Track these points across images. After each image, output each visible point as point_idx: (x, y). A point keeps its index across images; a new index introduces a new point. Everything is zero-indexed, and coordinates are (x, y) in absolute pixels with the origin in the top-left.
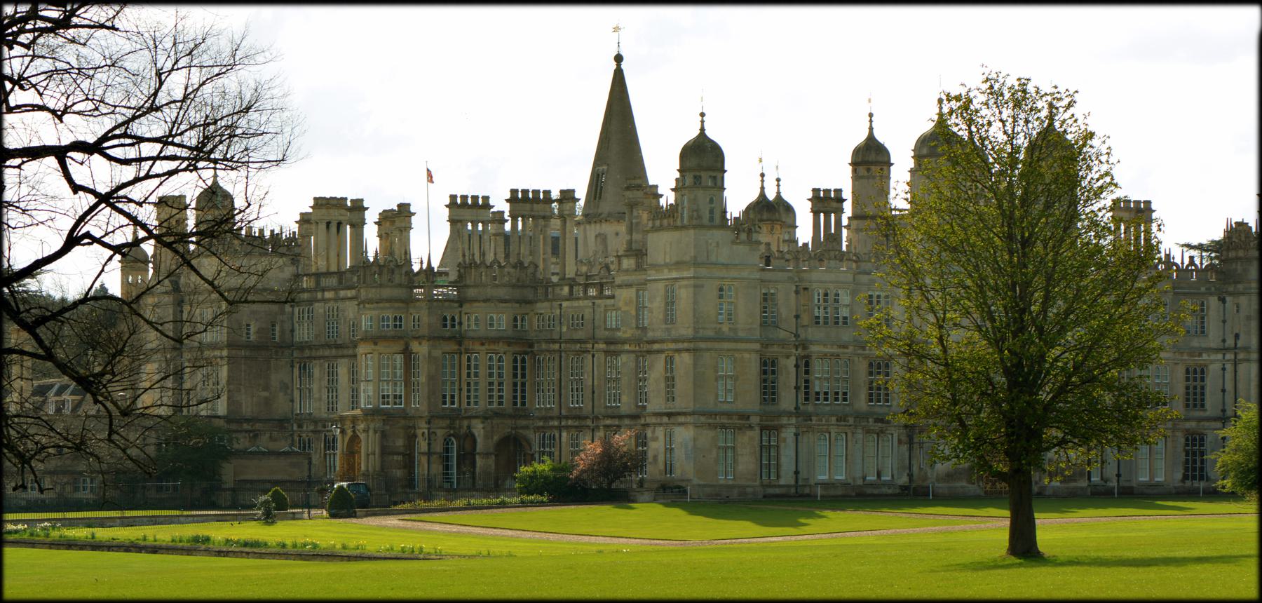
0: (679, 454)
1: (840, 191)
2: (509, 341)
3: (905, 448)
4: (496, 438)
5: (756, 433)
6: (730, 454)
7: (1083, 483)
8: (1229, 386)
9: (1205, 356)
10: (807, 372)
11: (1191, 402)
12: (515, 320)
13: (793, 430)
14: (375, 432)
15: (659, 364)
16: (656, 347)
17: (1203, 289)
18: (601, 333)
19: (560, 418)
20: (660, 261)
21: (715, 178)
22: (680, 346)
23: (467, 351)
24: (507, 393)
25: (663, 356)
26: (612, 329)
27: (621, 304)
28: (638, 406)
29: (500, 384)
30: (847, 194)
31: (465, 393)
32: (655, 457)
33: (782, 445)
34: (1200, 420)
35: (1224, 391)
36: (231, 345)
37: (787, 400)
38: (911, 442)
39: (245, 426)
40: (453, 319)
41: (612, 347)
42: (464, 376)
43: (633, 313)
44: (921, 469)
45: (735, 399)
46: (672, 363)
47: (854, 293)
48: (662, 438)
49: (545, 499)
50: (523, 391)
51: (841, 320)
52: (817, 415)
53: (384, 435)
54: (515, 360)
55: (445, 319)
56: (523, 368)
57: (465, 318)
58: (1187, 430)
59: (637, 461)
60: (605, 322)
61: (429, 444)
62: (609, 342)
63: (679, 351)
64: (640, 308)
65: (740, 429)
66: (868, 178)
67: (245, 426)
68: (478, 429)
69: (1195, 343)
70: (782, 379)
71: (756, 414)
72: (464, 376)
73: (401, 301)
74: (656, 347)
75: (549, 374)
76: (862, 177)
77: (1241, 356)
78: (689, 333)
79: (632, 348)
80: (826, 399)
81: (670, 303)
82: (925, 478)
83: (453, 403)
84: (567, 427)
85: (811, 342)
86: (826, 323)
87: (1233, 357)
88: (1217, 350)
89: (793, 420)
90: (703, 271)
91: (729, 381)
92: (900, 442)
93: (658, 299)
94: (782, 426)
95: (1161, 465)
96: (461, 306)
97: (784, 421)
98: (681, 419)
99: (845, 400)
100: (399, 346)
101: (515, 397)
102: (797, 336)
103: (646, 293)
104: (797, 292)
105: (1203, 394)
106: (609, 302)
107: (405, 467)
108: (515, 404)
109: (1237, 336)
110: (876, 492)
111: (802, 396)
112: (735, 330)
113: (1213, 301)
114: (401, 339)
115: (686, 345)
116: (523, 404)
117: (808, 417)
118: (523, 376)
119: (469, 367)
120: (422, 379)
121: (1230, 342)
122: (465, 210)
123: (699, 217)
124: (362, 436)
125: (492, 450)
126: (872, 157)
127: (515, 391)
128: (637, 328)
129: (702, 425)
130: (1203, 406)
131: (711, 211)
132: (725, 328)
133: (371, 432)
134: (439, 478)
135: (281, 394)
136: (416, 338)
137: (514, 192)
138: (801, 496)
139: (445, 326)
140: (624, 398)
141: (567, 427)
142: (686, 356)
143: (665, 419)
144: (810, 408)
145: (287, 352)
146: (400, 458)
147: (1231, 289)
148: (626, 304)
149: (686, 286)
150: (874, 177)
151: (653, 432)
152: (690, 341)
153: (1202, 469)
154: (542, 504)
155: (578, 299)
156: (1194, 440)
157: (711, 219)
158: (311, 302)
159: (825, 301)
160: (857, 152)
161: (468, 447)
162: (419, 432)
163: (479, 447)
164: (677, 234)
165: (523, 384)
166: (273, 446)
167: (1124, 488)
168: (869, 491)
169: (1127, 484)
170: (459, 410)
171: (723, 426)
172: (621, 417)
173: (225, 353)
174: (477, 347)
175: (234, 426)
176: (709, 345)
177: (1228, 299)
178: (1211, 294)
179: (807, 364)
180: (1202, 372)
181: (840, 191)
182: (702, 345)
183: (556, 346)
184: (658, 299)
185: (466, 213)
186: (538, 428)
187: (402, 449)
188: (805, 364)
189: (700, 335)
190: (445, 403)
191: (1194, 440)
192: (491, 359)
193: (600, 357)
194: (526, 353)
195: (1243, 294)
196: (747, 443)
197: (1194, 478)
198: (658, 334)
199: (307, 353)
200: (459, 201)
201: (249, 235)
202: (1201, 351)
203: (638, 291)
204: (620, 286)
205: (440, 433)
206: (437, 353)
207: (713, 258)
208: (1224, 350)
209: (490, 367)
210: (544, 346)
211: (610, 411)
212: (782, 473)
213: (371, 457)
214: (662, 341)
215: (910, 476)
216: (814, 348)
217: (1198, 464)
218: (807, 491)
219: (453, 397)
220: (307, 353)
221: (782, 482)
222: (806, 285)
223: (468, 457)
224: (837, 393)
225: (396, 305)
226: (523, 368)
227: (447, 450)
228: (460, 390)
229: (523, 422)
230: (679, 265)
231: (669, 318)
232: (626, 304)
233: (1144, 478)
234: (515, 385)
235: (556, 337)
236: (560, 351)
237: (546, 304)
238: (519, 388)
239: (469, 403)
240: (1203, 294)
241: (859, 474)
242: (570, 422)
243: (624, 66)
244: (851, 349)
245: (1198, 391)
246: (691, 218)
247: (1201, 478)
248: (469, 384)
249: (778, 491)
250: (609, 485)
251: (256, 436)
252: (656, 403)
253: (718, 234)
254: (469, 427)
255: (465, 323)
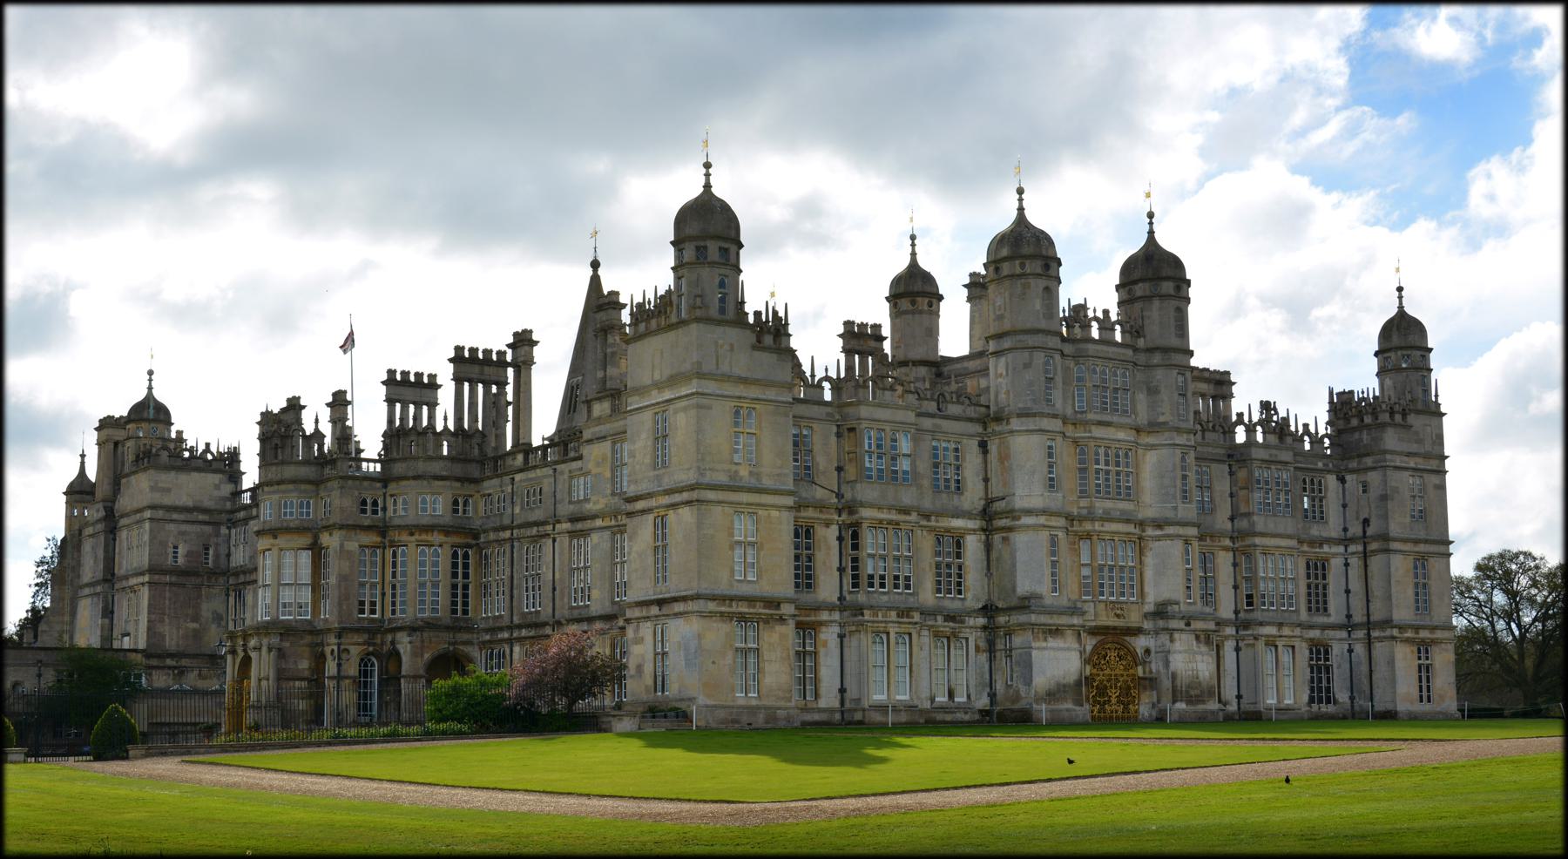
0: (676, 662)
1: (880, 326)
2: (446, 530)
3: (984, 657)
4: (427, 656)
5: (789, 629)
6: (751, 660)
7: (1213, 705)
8: (1356, 585)
9: (1326, 548)
10: (855, 547)
11: (1313, 605)
12: (456, 503)
13: (836, 629)
14: (270, 650)
15: (644, 531)
16: (640, 505)
17: (1320, 465)
18: (565, 509)
19: (510, 628)
20: (647, 381)
21: (726, 250)
22: (677, 498)
23: (393, 544)
24: (444, 598)
25: (651, 517)
26: (579, 502)
27: (591, 466)
28: (614, 603)
29: (435, 585)
30: (886, 331)
31: (388, 599)
32: (639, 668)
33: (822, 651)
34: (1324, 627)
35: (1348, 592)
36: (152, 570)
37: (828, 587)
38: (991, 649)
39: (169, 662)
40: (375, 503)
41: (579, 526)
42: (388, 577)
43: (608, 474)
44: (1008, 687)
45: (759, 577)
46: (664, 526)
47: (915, 440)
48: (649, 639)
49: (465, 728)
50: (465, 596)
51: (900, 475)
52: (871, 607)
53: (281, 654)
54: (455, 555)
55: (364, 502)
56: (466, 566)
57: (390, 501)
58: (1312, 640)
59: (613, 673)
60: (570, 493)
61: (339, 665)
62: (574, 519)
63: (674, 506)
64: (616, 466)
65: (766, 622)
66: (913, 313)
67: (169, 662)
68: (404, 644)
69: (1316, 531)
70: (820, 556)
71: (790, 601)
72: (388, 577)
73: (309, 482)
74: (640, 505)
75: (499, 570)
76: (906, 312)
77: (1374, 546)
78: (689, 477)
79: (607, 523)
80: (882, 585)
81: (661, 437)
82: (1017, 698)
83: (373, 612)
84: (520, 640)
85: (862, 505)
86: (880, 477)
87: (1360, 548)
88: (1338, 542)
89: (836, 616)
90: (710, 386)
91: (750, 551)
92: (977, 649)
93: (644, 436)
94: (821, 623)
95: (1288, 683)
96: (385, 487)
97: (824, 616)
98: (679, 607)
99: (908, 587)
100: (306, 540)
101: (454, 603)
102: (839, 495)
103: (626, 446)
104: (839, 435)
105: (1325, 595)
106: (575, 465)
107: (311, 696)
108: (454, 612)
109: (1366, 522)
110: (948, 718)
111: (848, 580)
112: (757, 475)
113: (1331, 480)
114: (311, 535)
115: (685, 496)
116: (465, 612)
117: (859, 610)
118: (466, 576)
119: (394, 565)
120: (333, 580)
121: (1355, 530)
122: (407, 389)
123: (705, 306)
124: (253, 655)
125: (422, 672)
126: (918, 286)
127: (455, 595)
128: (613, 494)
129: (710, 615)
130: (1326, 610)
131: (722, 300)
132: (744, 472)
133: (264, 649)
134: (352, 712)
135: (214, 626)
136: (328, 528)
137: (459, 349)
138: (850, 723)
139: (364, 511)
140: (595, 594)
141: (520, 640)
142: (686, 513)
143: (654, 610)
144: (861, 598)
145: (221, 580)
146: (304, 684)
147: (1353, 464)
148: (598, 465)
149: (685, 409)
150: (921, 312)
151: (637, 630)
152: (692, 488)
153: (1328, 690)
154: (459, 735)
155: (535, 467)
156: (1318, 652)
157: (722, 311)
158: (246, 521)
159: (879, 446)
160: (897, 282)
161: (392, 668)
162: (328, 650)
163: (405, 669)
164: (672, 335)
165: (466, 587)
166: (201, 684)
167: (1247, 713)
168: (939, 717)
169: (1251, 708)
170: (382, 621)
171: (742, 618)
172: (590, 620)
173: (146, 578)
174: (405, 537)
175: (154, 662)
176: (721, 496)
177: (1348, 477)
178: (1329, 472)
179: (855, 536)
180: (1324, 568)
181: (880, 326)
182: (711, 495)
183: (507, 534)
184: (644, 436)
185: (408, 393)
186: (484, 643)
187: (306, 674)
188: (852, 536)
189: (706, 480)
190: (362, 612)
191: (1318, 652)
192: (423, 553)
193: (563, 541)
194: (470, 546)
195: (1374, 469)
196: (779, 642)
197: (1320, 701)
198: (644, 487)
199: (242, 579)
200: (398, 377)
201: (192, 457)
202: (1321, 542)
203: (614, 443)
204: (589, 441)
205: (355, 651)
206: (352, 546)
207: (725, 368)
208: (1346, 541)
209: (422, 564)
210: (492, 536)
211: (576, 613)
212: (823, 690)
213: (264, 683)
214: (650, 495)
215: (992, 696)
216: (866, 513)
217: (1324, 683)
218: (858, 716)
219: (373, 604)
220: (242, 579)
221: (822, 704)
222: (853, 423)
223: (391, 680)
224: (896, 578)
225: (303, 487)
226: (466, 566)
227: (365, 674)
228: (383, 594)
229: (465, 636)
230: (673, 380)
231: (660, 461)
232: (598, 465)
233: (1272, 701)
234: (455, 587)
235: (507, 521)
236: (511, 540)
237: (496, 481)
238: (460, 591)
239: (394, 612)
240: (1321, 471)
241: (925, 694)
242: (524, 633)
243: (601, 272)
244: (914, 517)
245: (1320, 590)
246: (693, 307)
247: (1328, 701)
248: (394, 587)
249: (817, 717)
250: (565, 702)
251: (182, 673)
252: (641, 588)
253: (733, 334)
254: (393, 643)
255: (390, 508)
